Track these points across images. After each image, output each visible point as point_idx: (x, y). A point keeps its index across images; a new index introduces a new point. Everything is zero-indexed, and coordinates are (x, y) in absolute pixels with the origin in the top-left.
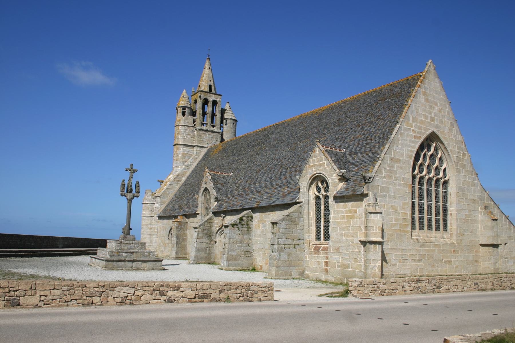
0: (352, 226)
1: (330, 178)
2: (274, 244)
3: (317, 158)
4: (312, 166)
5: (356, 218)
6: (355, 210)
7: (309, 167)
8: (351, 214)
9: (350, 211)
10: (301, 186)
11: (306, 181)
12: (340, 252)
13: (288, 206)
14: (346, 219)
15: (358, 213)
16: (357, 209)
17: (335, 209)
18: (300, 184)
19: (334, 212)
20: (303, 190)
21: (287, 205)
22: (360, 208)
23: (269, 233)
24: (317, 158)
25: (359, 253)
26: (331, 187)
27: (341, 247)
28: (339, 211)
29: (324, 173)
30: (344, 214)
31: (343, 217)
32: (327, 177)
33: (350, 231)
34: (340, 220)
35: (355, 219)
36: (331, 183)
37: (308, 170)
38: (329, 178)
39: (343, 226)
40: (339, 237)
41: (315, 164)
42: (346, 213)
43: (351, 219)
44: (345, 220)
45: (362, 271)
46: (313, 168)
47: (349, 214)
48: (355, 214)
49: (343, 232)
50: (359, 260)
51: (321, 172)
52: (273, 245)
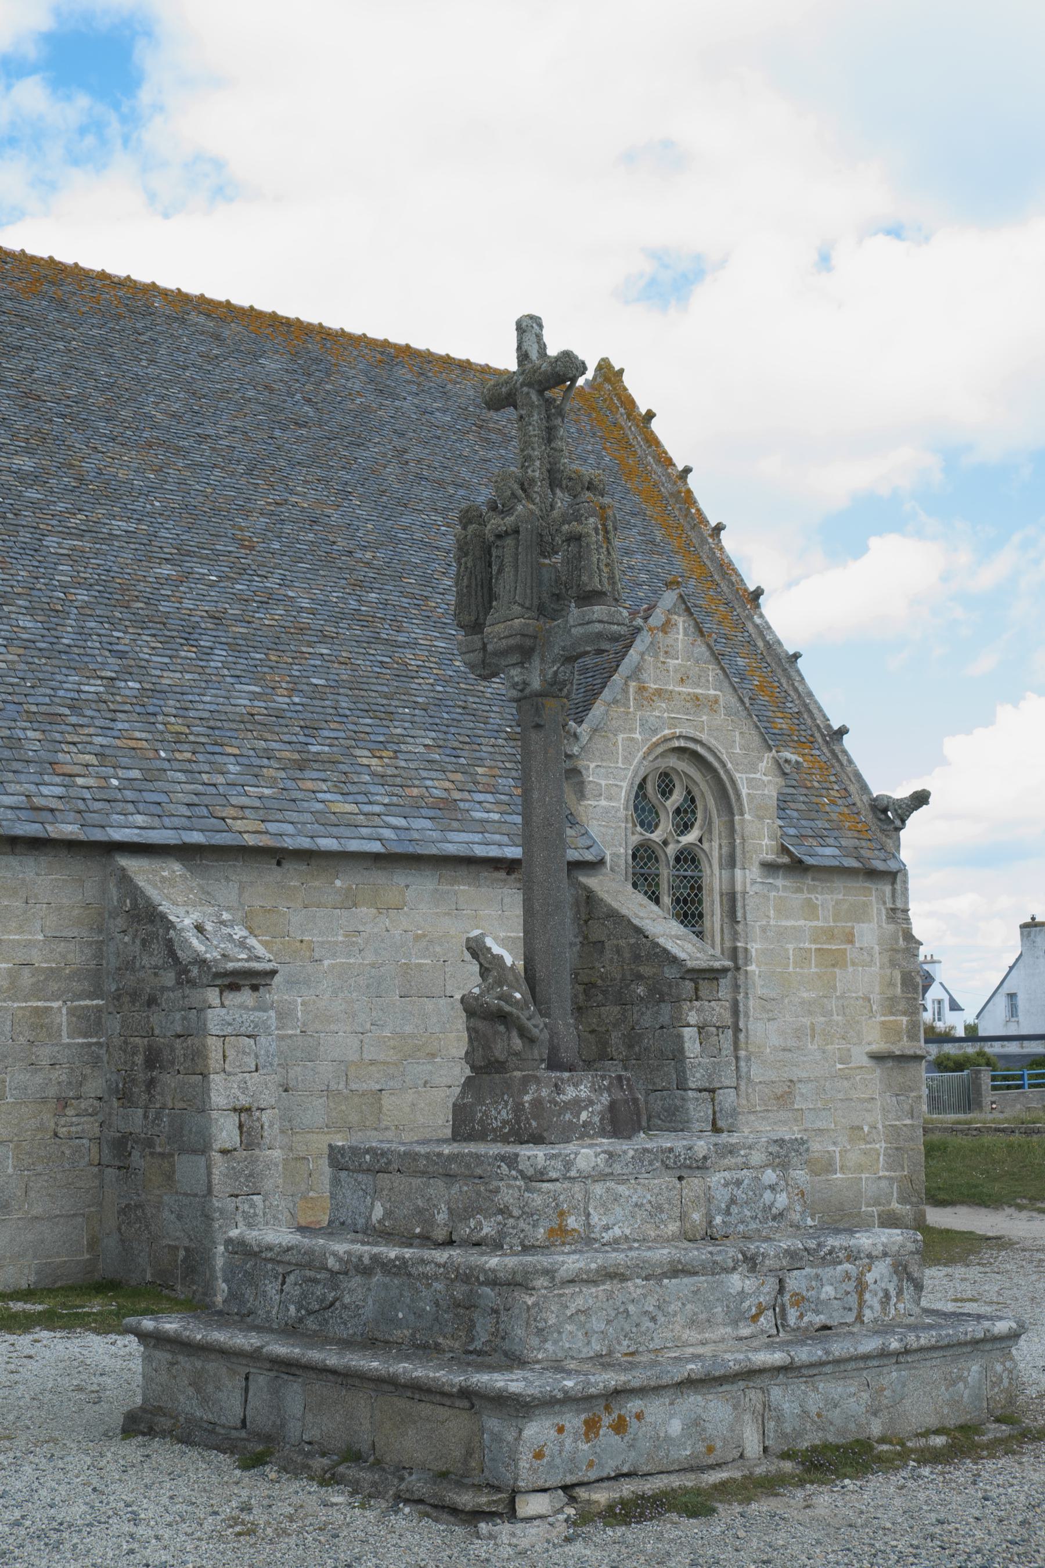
0: (838, 994)
1: (744, 776)
2: (718, 1085)
3: (679, 661)
4: (659, 692)
5: (853, 964)
6: (847, 930)
7: (642, 689)
8: (834, 948)
9: (830, 934)
10: (591, 779)
11: (627, 760)
12: (796, 1107)
13: (502, 875)
14: (816, 966)
15: (857, 945)
16: (853, 928)
17: (768, 917)
18: (587, 768)
19: (764, 930)
20: (603, 803)
21: (497, 869)
22: (864, 926)
23: (333, 1027)
24: (679, 661)
25: (869, 1106)
26: (747, 816)
27: (799, 1085)
28: (786, 928)
29: (713, 742)
30: (807, 945)
31: (803, 956)
32: (729, 765)
33: (835, 1017)
34: (791, 969)
35: (850, 969)
36: (750, 801)
37: (640, 707)
38: (737, 776)
39: (805, 995)
40: (791, 1043)
41: (671, 688)
42: (814, 941)
43: (833, 965)
44: (814, 970)
45: (881, 1174)
46: (664, 705)
47: (829, 947)
48: (850, 946)
49: (806, 1021)
50: (869, 1132)
51: (703, 737)
52: (712, 1091)
